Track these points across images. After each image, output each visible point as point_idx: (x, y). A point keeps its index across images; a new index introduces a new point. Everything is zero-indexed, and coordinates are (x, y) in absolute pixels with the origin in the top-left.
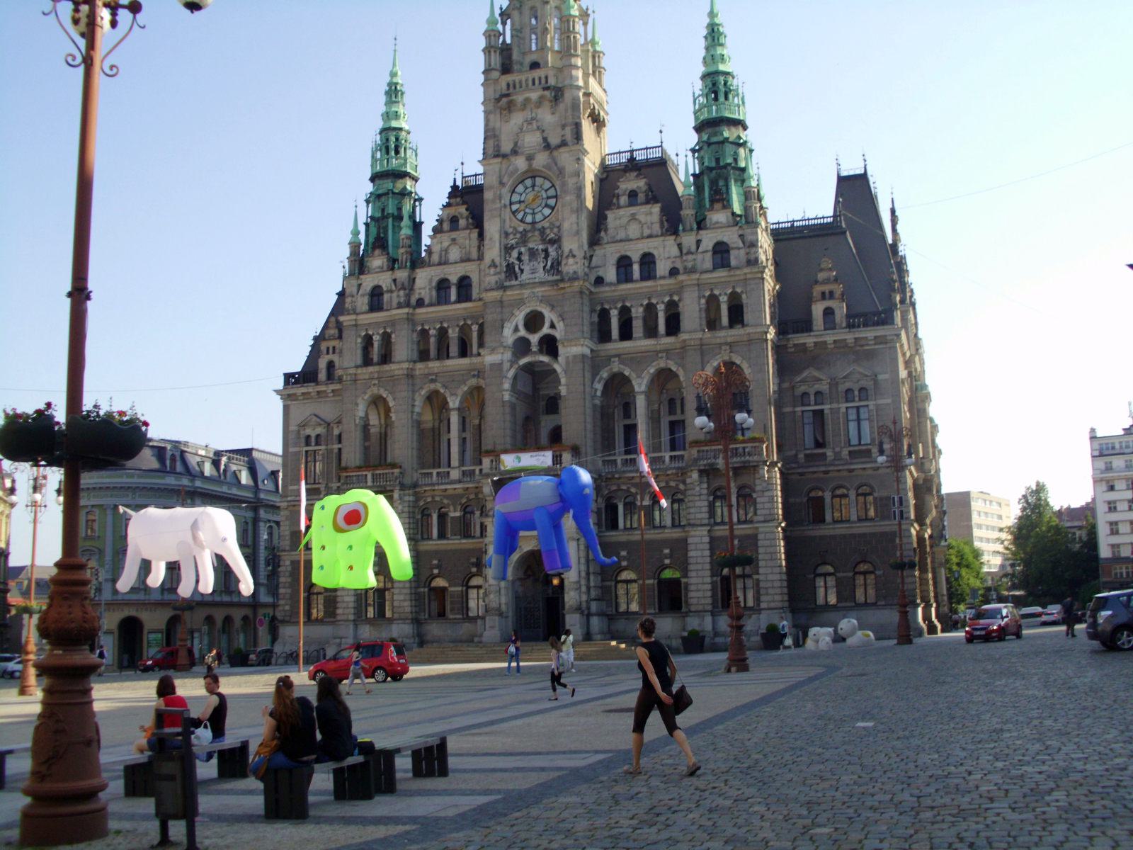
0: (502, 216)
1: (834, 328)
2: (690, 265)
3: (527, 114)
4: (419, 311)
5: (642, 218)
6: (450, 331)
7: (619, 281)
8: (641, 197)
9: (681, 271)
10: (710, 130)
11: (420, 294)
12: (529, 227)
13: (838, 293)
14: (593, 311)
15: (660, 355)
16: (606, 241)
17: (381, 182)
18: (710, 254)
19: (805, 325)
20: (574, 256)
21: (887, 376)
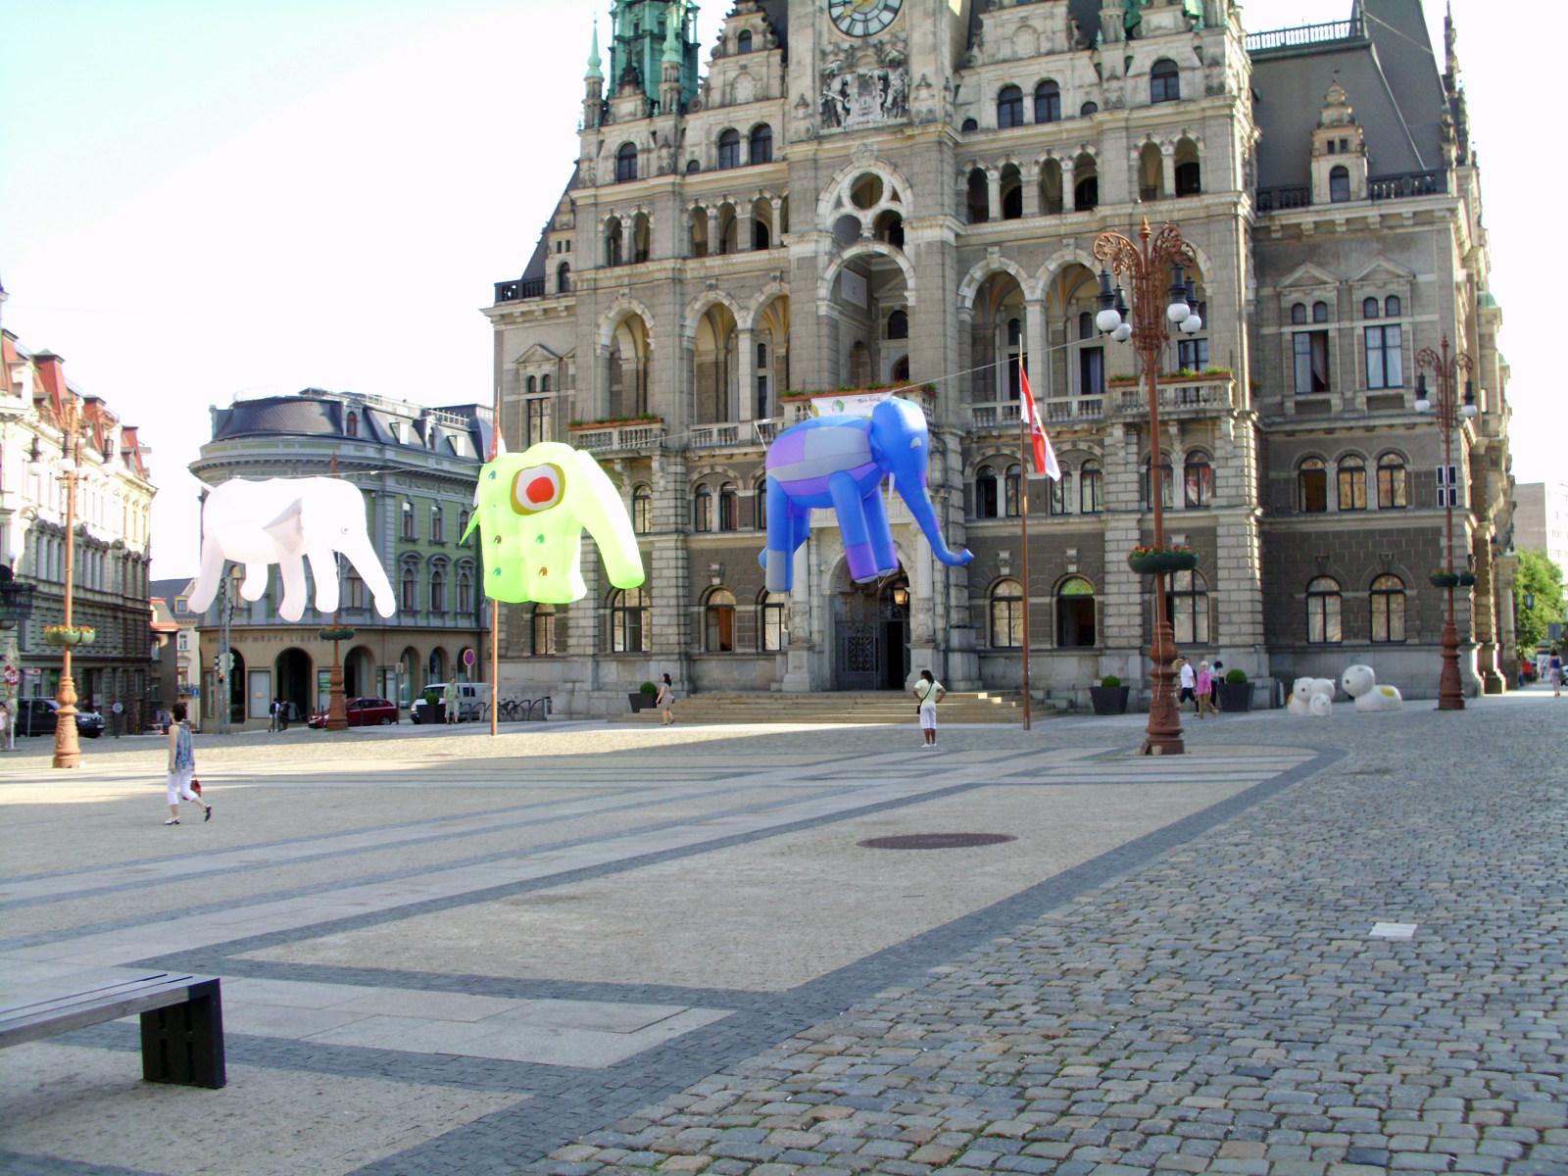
0: (817, 26)
1: (1348, 200)
2: (1113, 97)
4: (691, 179)
5: (1037, 23)
6: (738, 209)
7: (1001, 126)
9: (1100, 106)
11: (693, 153)
12: (858, 43)
13: (1354, 144)
14: (959, 173)
15: (1065, 241)
16: (980, 62)
18: (1147, 78)
19: (1301, 196)
20: (929, 86)
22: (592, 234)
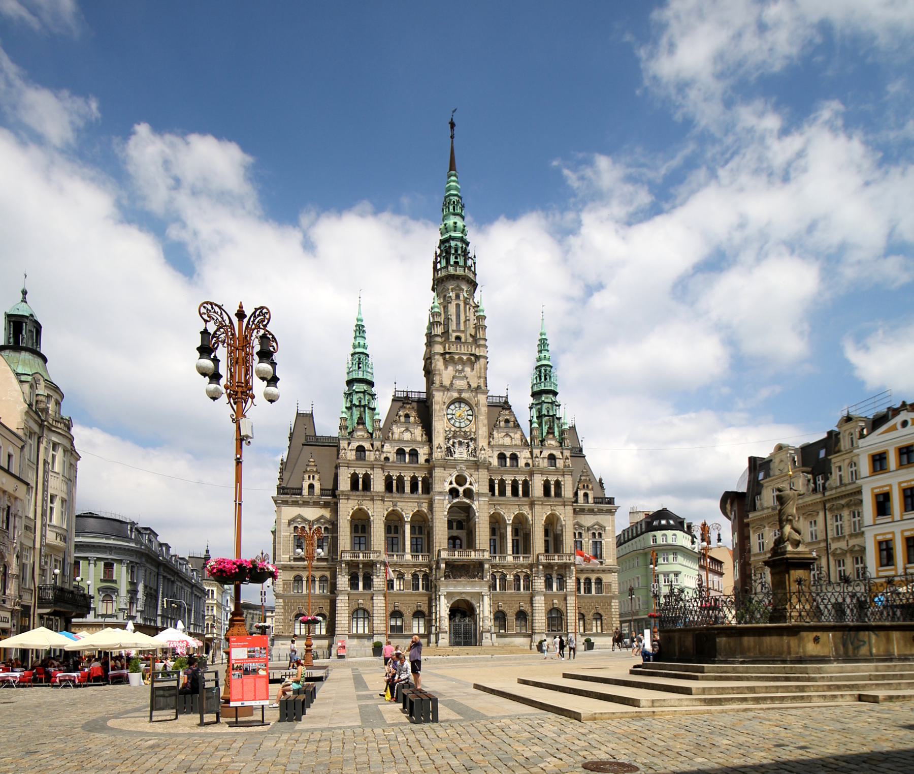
3: (460, 367)
5: (512, 435)
6: (405, 478)
8: (511, 424)
9: (531, 466)
10: (544, 395)
12: (458, 430)
17: (358, 384)
18: (546, 460)
20: (484, 450)
21: (610, 528)
22: (346, 478)
